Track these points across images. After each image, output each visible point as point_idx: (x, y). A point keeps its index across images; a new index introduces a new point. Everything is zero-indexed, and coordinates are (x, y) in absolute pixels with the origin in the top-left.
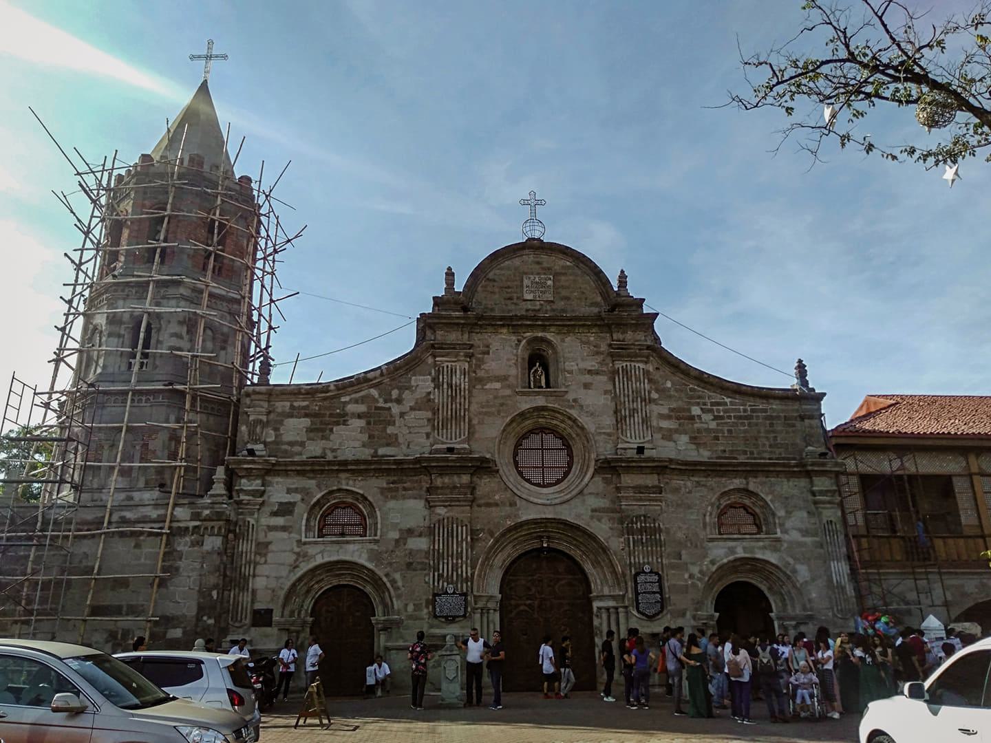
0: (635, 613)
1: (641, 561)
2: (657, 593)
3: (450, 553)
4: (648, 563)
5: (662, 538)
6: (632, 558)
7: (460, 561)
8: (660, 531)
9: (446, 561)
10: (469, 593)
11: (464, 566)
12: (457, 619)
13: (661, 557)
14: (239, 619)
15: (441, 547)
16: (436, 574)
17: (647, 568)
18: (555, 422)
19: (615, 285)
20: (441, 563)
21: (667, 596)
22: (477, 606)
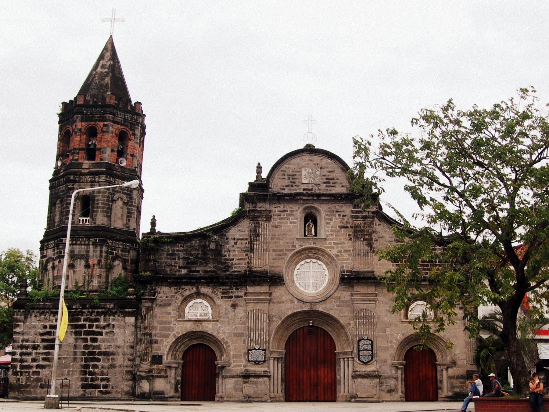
0: (357, 361)
1: (362, 334)
2: (370, 350)
4: (366, 335)
6: (357, 332)
7: (262, 332)
8: (374, 317)
10: (267, 349)
11: (265, 335)
12: (261, 363)
13: (374, 331)
15: (252, 325)
16: (249, 339)
20: (252, 333)
21: (375, 352)
22: (271, 356)
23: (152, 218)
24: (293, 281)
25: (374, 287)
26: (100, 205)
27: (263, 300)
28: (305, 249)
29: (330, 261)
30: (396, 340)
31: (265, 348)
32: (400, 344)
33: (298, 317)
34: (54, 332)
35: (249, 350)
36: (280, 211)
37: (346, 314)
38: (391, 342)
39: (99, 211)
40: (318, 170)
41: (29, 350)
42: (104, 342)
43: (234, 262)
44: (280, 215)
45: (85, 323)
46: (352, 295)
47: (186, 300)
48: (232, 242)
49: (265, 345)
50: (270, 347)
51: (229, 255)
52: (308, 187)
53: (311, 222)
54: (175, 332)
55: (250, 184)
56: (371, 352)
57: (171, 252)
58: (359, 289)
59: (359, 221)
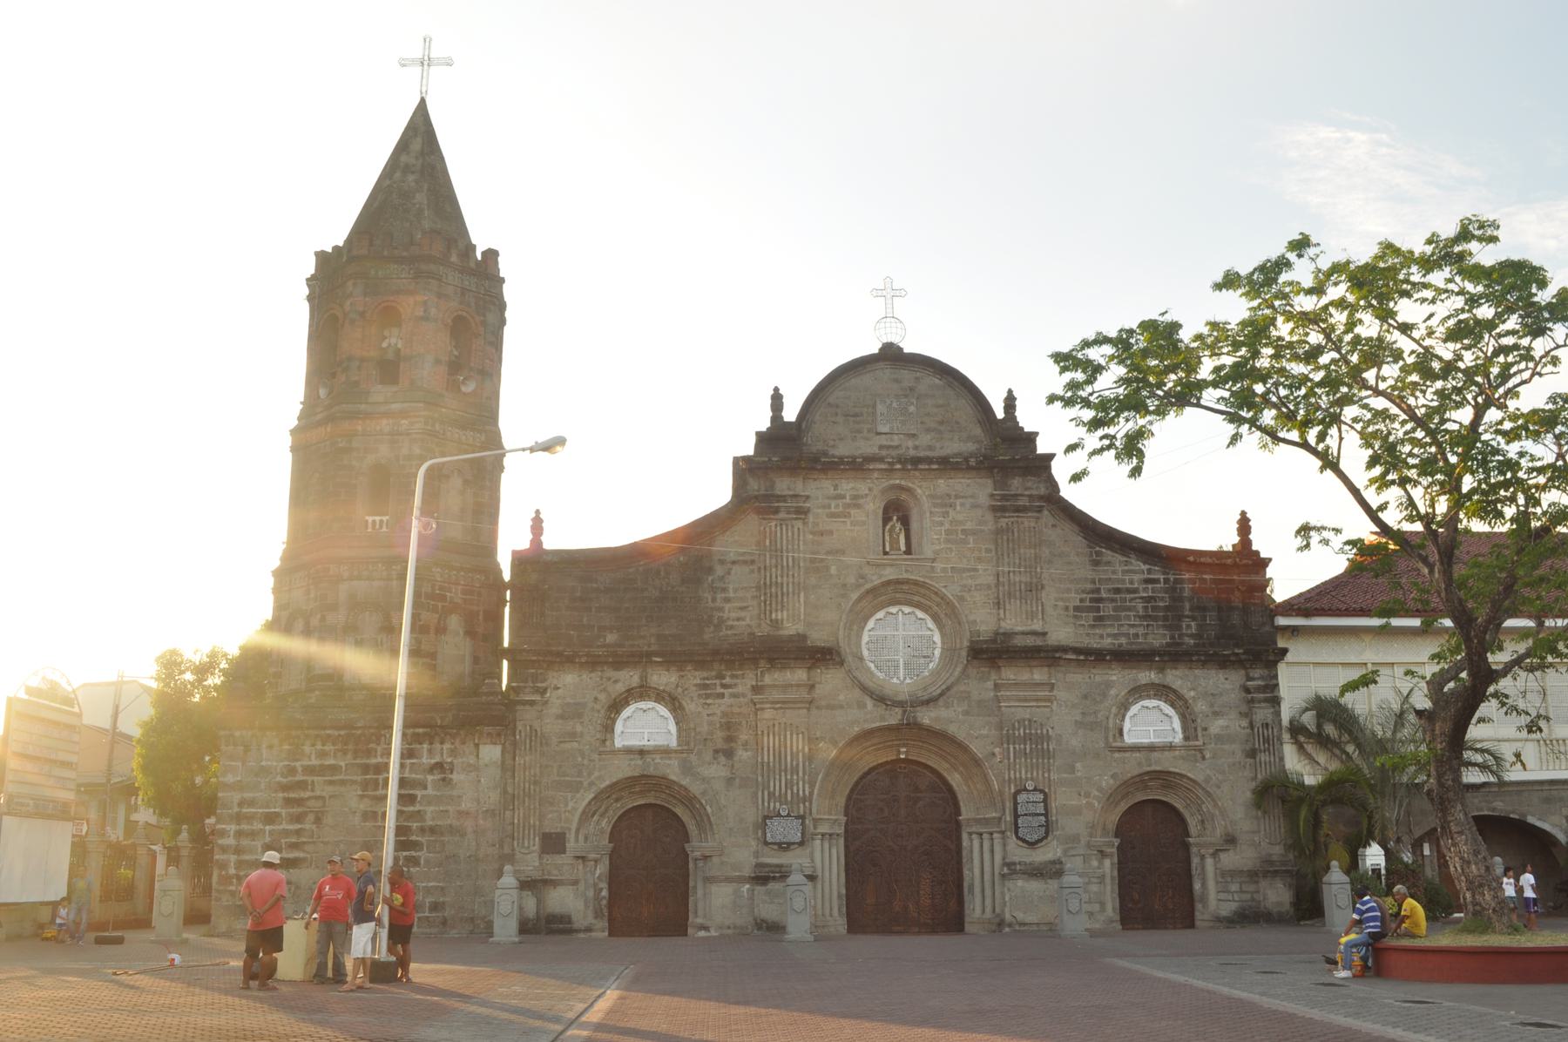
1: (1024, 777)
2: (1042, 815)
3: (783, 767)
4: (1032, 779)
5: (1051, 748)
6: (1012, 772)
7: (795, 777)
8: (1049, 738)
11: (801, 783)
12: (792, 847)
13: (1049, 771)
14: (526, 845)
16: (766, 793)
17: (1030, 787)
19: (1000, 414)
21: (1054, 818)
22: (819, 831)
23: (534, 515)
24: (861, 659)
25: (1046, 669)
28: (889, 583)
29: (943, 611)
30: (1100, 789)
31: (802, 813)
32: (1108, 799)
33: (875, 741)
34: (313, 782)
36: (829, 498)
37: (985, 732)
38: (1087, 795)
40: (912, 404)
41: (257, 826)
42: (429, 804)
43: (726, 616)
44: (829, 507)
46: (997, 687)
48: (719, 570)
49: (801, 805)
50: (814, 810)
51: (714, 600)
52: (892, 440)
53: (897, 520)
55: (759, 434)
56: (1043, 818)
57: (578, 594)
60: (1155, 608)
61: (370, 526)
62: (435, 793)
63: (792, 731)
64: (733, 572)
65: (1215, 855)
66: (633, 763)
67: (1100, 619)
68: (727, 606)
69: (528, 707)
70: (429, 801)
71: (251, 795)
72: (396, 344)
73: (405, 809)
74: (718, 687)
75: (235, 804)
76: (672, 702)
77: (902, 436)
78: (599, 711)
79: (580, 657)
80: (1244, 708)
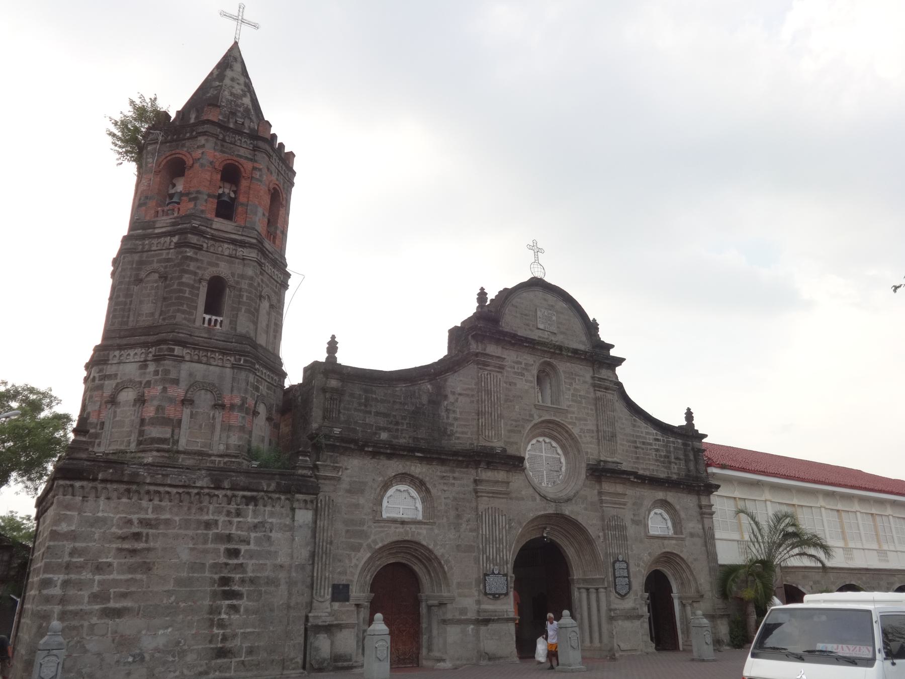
2: (626, 577)
3: (494, 538)
7: (501, 546)
9: (491, 545)
12: (501, 597)
14: (322, 594)
15: (488, 533)
18: (555, 434)
26: (245, 299)
27: (500, 494)
34: (147, 534)
35: (486, 575)
37: (594, 522)
39: (243, 310)
42: (251, 557)
45: (216, 518)
46: (600, 493)
47: (386, 486)
48: (451, 398)
51: (448, 418)
54: (370, 540)
58: (607, 487)
59: (601, 391)
60: (660, 456)
61: (206, 322)
62: (256, 548)
63: (499, 513)
64: (459, 400)
65: (691, 604)
66: (397, 530)
67: (638, 458)
68: (456, 423)
69: (327, 482)
70: (251, 555)
71: (84, 545)
72: (229, 194)
73: (230, 562)
74: (451, 479)
75: (67, 553)
76: (420, 484)
77: (549, 333)
78: (375, 490)
79: (368, 446)
80: (699, 518)
